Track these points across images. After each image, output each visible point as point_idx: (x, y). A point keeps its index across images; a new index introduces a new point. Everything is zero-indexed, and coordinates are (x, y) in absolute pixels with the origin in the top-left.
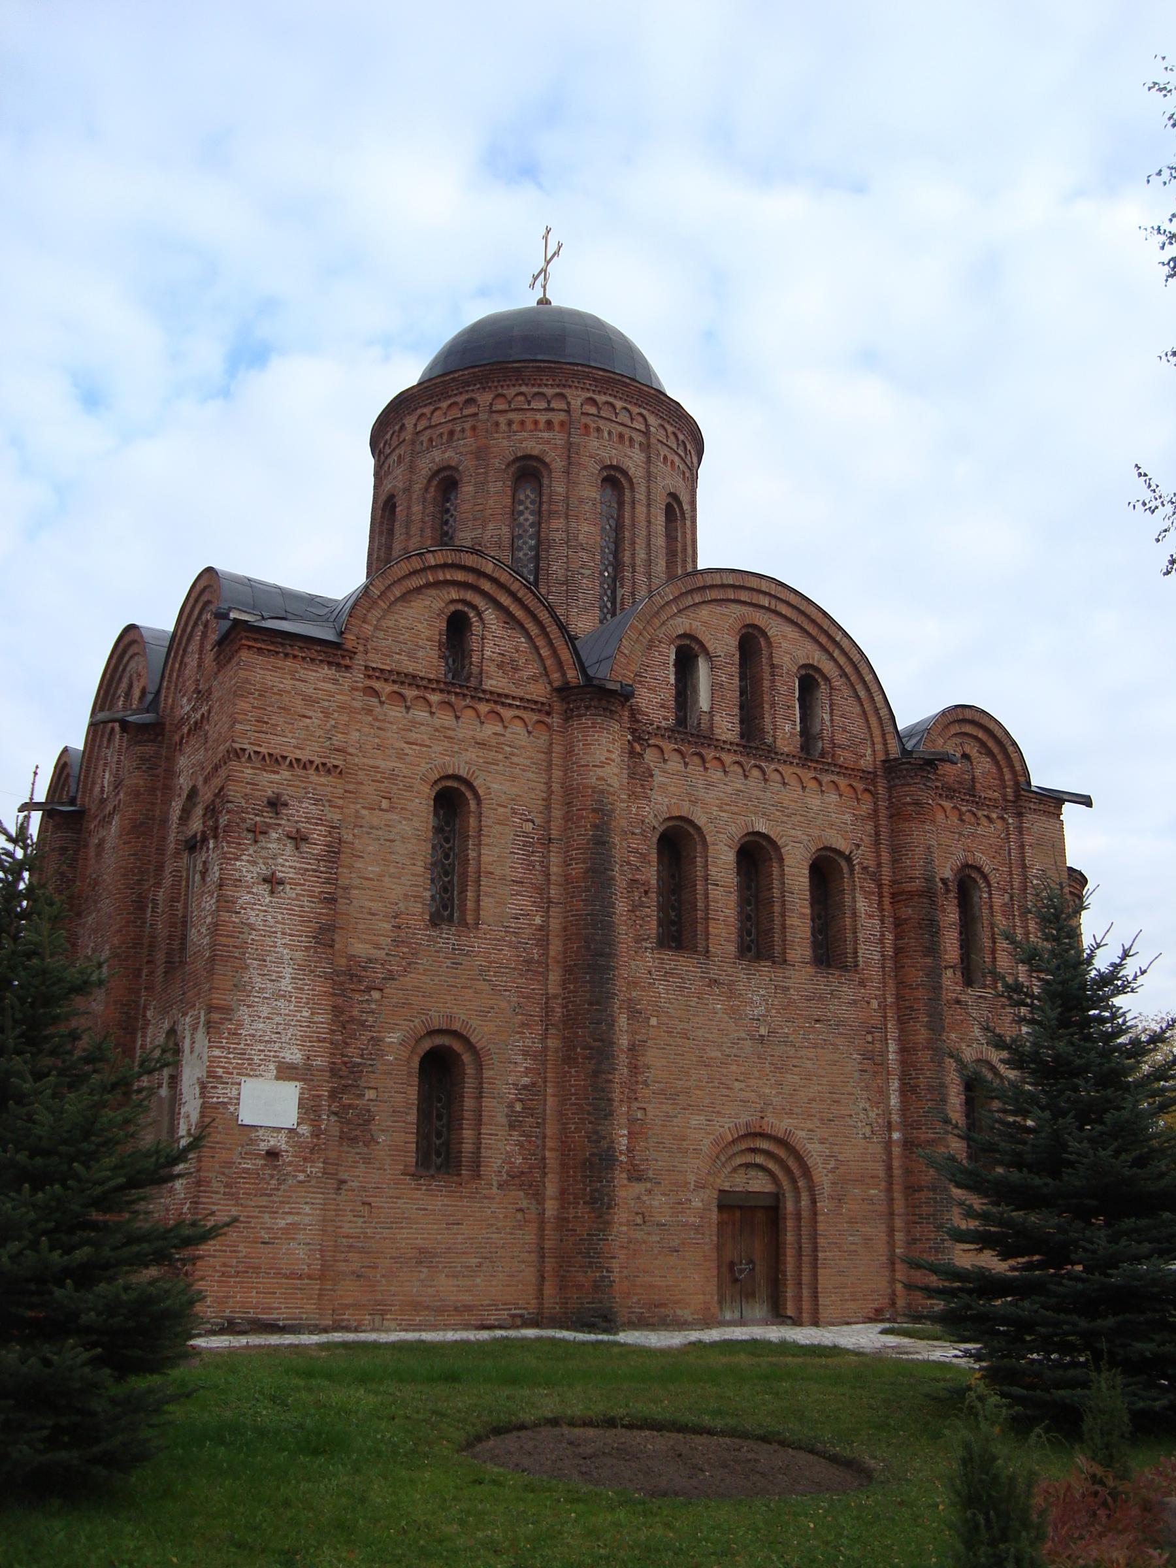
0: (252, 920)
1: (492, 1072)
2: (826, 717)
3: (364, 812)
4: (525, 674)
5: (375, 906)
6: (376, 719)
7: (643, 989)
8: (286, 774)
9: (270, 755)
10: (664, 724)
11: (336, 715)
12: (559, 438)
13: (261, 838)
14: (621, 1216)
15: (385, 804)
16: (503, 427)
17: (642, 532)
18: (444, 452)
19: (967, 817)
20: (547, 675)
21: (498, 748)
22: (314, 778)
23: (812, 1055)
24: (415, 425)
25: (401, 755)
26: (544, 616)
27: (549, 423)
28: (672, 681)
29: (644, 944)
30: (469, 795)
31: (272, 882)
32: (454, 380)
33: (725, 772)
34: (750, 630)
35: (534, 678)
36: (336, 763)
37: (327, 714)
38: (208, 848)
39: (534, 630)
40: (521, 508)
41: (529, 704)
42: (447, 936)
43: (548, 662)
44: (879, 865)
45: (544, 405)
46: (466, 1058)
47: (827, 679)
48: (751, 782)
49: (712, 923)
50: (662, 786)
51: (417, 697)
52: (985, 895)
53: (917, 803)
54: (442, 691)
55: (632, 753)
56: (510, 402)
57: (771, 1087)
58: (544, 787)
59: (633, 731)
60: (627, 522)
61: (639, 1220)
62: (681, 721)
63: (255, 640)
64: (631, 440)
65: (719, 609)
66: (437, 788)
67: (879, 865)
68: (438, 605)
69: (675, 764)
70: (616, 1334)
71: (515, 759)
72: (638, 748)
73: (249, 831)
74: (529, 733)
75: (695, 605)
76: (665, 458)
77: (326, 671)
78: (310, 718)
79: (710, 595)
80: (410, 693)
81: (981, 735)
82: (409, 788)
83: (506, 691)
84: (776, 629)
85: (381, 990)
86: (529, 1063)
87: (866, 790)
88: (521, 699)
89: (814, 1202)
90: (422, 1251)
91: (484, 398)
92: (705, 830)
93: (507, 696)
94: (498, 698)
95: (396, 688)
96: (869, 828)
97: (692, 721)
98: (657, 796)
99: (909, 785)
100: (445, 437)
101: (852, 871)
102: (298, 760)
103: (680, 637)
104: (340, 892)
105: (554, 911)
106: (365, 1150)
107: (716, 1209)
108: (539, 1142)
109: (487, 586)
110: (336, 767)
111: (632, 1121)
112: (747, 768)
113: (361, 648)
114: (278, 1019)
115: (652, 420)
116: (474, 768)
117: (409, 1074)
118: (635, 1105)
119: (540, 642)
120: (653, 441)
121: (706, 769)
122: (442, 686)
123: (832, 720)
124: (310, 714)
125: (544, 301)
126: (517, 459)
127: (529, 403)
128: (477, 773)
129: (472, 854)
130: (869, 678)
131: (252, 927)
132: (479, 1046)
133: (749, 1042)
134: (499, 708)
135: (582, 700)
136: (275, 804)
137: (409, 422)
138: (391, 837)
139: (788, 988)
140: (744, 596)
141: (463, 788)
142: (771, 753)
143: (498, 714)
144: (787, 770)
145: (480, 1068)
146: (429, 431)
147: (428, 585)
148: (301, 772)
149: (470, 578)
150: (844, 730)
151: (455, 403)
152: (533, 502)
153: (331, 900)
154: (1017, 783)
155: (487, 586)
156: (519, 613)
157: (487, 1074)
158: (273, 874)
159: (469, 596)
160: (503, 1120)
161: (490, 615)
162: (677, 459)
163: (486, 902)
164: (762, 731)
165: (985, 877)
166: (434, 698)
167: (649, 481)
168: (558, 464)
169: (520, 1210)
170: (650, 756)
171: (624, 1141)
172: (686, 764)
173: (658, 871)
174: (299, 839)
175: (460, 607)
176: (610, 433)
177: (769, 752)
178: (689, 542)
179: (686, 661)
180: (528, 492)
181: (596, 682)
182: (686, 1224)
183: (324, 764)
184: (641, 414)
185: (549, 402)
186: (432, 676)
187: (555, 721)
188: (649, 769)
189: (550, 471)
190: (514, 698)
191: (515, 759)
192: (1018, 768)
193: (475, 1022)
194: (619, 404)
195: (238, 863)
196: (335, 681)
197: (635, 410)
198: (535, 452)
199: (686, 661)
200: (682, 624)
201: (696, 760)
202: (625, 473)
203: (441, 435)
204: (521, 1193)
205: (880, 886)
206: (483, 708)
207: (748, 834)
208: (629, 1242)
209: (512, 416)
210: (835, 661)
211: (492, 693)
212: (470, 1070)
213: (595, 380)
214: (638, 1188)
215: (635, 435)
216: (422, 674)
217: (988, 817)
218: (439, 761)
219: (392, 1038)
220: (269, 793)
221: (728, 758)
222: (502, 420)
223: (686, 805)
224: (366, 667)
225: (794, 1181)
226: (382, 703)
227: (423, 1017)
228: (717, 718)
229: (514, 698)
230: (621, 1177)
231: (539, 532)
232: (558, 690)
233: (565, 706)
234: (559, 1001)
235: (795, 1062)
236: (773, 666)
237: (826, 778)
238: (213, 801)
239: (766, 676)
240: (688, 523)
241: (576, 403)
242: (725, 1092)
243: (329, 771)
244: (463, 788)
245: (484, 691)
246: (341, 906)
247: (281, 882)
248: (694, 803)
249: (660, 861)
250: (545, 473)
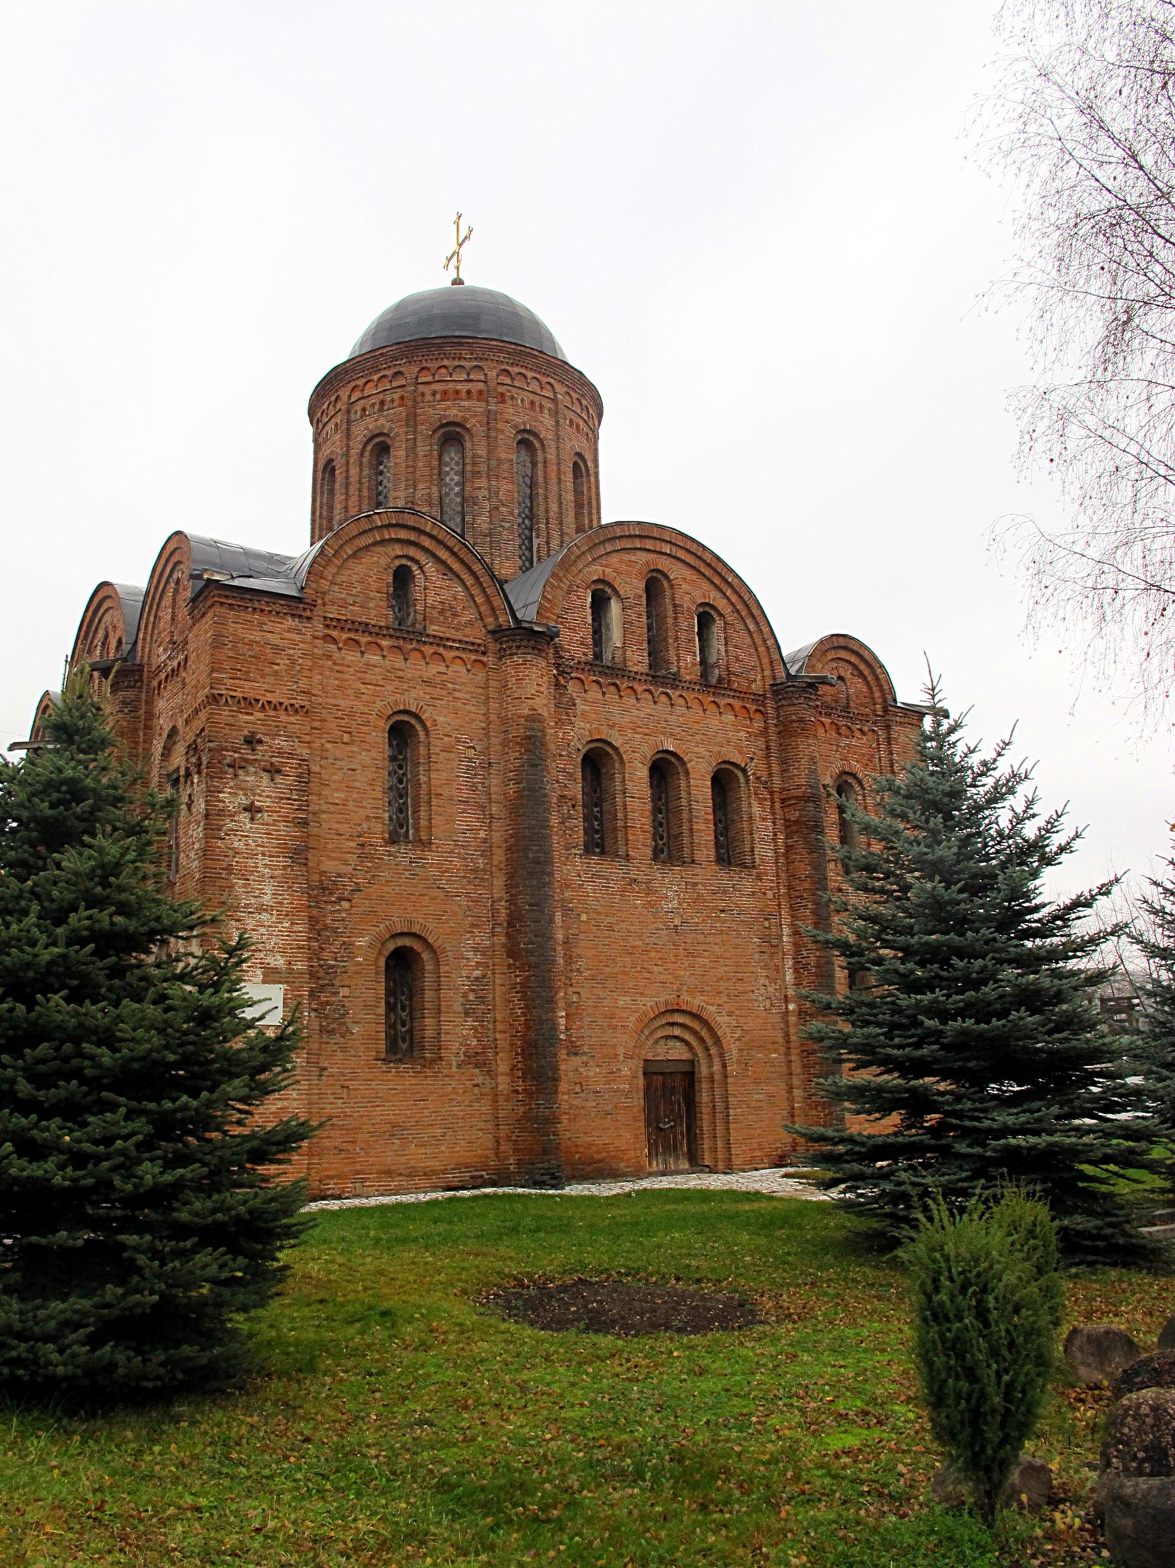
0: (236, 844)
1: (447, 968)
2: (723, 649)
3: (329, 746)
4: (463, 620)
5: (342, 828)
6: (335, 664)
7: (573, 890)
8: (261, 715)
9: (245, 698)
10: (583, 659)
11: (301, 661)
12: (479, 407)
13: (241, 772)
14: (563, 1086)
15: (346, 738)
16: (428, 397)
17: (553, 487)
18: (376, 420)
19: (843, 730)
20: (482, 619)
21: (443, 686)
22: (283, 718)
23: (718, 941)
24: (350, 396)
25: (358, 694)
26: (477, 567)
28: (590, 621)
29: (573, 851)
30: (418, 727)
32: (382, 355)
33: (637, 699)
34: (655, 574)
35: (470, 623)
36: (302, 703)
37: (293, 662)
38: (192, 783)
39: (469, 581)
40: (447, 469)
41: (469, 647)
42: (403, 853)
43: (482, 608)
44: (770, 775)
45: (465, 377)
46: (425, 956)
47: (721, 615)
48: (659, 707)
49: (630, 831)
50: (584, 715)
51: (370, 643)
52: (860, 798)
53: (801, 720)
54: (391, 636)
55: (557, 684)
57: (685, 969)
58: (482, 718)
59: (558, 666)
60: (541, 480)
61: (578, 1089)
62: (598, 656)
63: (227, 597)
64: (541, 406)
65: (627, 557)
66: (391, 722)
67: (770, 775)
68: (384, 561)
69: (594, 693)
70: (563, 1189)
71: (457, 694)
72: (562, 681)
73: (229, 766)
74: (468, 671)
75: (607, 554)
76: (571, 421)
77: (290, 622)
78: (278, 664)
79: (618, 545)
80: (364, 639)
81: (853, 659)
82: (367, 723)
83: (448, 635)
84: (676, 572)
85: (350, 900)
86: (479, 958)
87: (757, 710)
88: (460, 642)
89: (724, 1066)
90: (394, 1125)
92: (622, 750)
93: (448, 639)
94: (440, 641)
95: (352, 635)
96: (761, 743)
97: (607, 656)
98: (580, 723)
99: (794, 705)
100: (377, 407)
101: (747, 781)
102: (269, 702)
103: (595, 582)
104: (311, 817)
105: (496, 825)
106: (342, 1040)
107: (641, 1076)
108: (491, 1026)
109: (427, 542)
110: (302, 707)
111: (569, 1004)
112: (656, 695)
113: (320, 602)
114: (262, 930)
115: (559, 388)
116: (422, 704)
117: (377, 973)
118: (570, 990)
119: (475, 591)
120: (561, 406)
121: (621, 697)
122: (391, 632)
123: (726, 651)
124: (278, 661)
125: (458, 282)
126: (443, 426)
128: (425, 707)
129: (423, 779)
130: (755, 612)
131: (237, 853)
132: (435, 945)
133: (665, 932)
134: (441, 650)
135: (514, 641)
136: (251, 741)
137: (344, 394)
138: (353, 767)
139: (696, 884)
140: (649, 545)
141: (413, 721)
142: (674, 681)
143: (440, 655)
144: (689, 696)
145: (437, 963)
146: (362, 401)
147: (375, 544)
148: (272, 713)
149: (412, 536)
150: (738, 660)
151: (384, 376)
152: (457, 464)
153: (305, 823)
154: (885, 700)
155: (427, 542)
156: (456, 566)
157: (443, 969)
158: (253, 803)
159: (412, 551)
160: (460, 1009)
161: (430, 567)
162: (581, 423)
163: (436, 820)
164: (668, 662)
165: (860, 782)
166: (385, 643)
167: (558, 442)
168: (479, 430)
169: (477, 1085)
170: (572, 688)
171: (563, 1021)
172: (604, 693)
173: (583, 787)
174: (273, 771)
175: (404, 562)
176: (522, 400)
177: (674, 680)
178: (594, 496)
179: (600, 603)
180: (453, 455)
181: (524, 625)
182: (618, 1090)
183: (292, 705)
184: (549, 383)
185: (468, 374)
186: (383, 624)
187: (489, 659)
188: (572, 699)
189: (472, 436)
190: (454, 641)
191: (457, 694)
192: (886, 687)
193: (431, 926)
194: (530, 374)
195: (221, 795)
196: (299, 631)
197: (545, 380)
198: (458, 420)
199: (600, 603)
200: (596, 571)
201: (612, 689)
202: (536, 435)
203: (373, 404)
204: (477, 1070)
205: (772, 793)
206: (428, 650)
207: (659, 752)
208: (570, 1108)
210: (728, 598)
211: (434, 637)
212: (429, 967)
213: (508, 353)
214: (576, 1061)
215: (545, 402)
216: (373, 622)
217: (860, 730)
218: (391, 699)
219: (361, 942)
220: (246, 732)
221: (639, 688)
223: (605, 729)
224: (325, 618)
225: (707, 1049)
226: (340, 649)
227: (387, 923)
228: (629, 653)
229: (454, 641)
230: (562, 1054)
231: (463, 490)
232: (492, 632)
233: (499, 646)
234: (503, 903)
235: (704, 947)
236: (675, 606)
237: (723, 702)
238: (195, 741)
239: (670, 614)
240: (592, 479)
241: (492, 374)
242: (646, 975)
243: (296, 711)
244: (413, 721)
245: (428, 636)
246: (313, 829)
247: (259, 810)
248: (611, 727)
249: (584, 778)
250: (467, 438)
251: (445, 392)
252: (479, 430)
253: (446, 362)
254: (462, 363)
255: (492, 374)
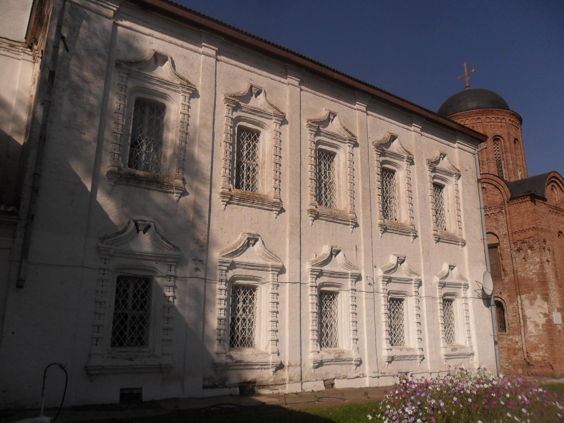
27: (501, 126)
31: (548, 261)
32: (472, 112)
45: (500, 121)
56: (490, 120)
91: (483, 118)
109: (558, 181)
127: (496, 120)
136: (544, 241)
155: (558, 181)
185: (501, 120)
209: (491, 123)
222: (489, 124)
251: (494, 126)
252: (506, 138)
253: (494, 116)
254: (499, 117)
255: (507, 121)
